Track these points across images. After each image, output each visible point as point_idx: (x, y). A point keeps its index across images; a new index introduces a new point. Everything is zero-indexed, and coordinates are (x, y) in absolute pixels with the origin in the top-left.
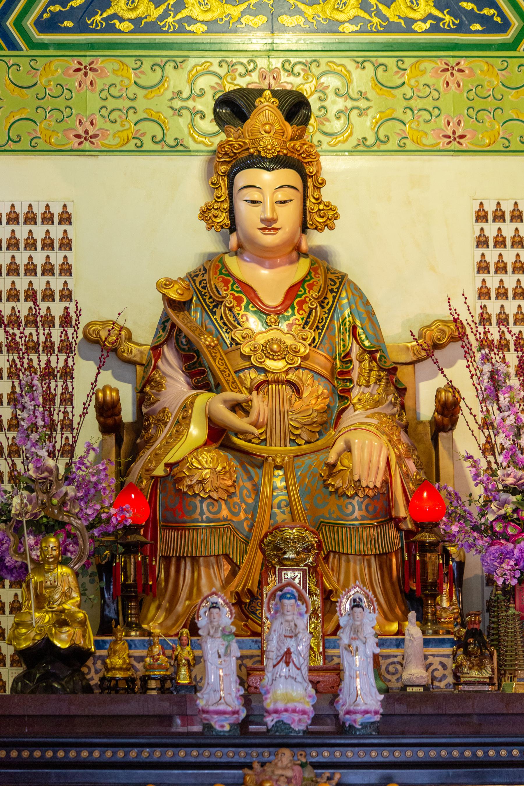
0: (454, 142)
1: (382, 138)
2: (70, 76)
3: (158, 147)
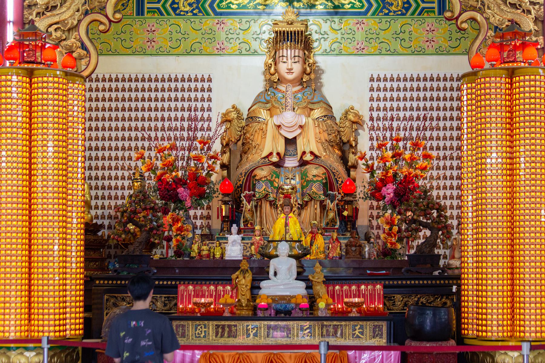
0: (360, 52)
3: (248, 53)
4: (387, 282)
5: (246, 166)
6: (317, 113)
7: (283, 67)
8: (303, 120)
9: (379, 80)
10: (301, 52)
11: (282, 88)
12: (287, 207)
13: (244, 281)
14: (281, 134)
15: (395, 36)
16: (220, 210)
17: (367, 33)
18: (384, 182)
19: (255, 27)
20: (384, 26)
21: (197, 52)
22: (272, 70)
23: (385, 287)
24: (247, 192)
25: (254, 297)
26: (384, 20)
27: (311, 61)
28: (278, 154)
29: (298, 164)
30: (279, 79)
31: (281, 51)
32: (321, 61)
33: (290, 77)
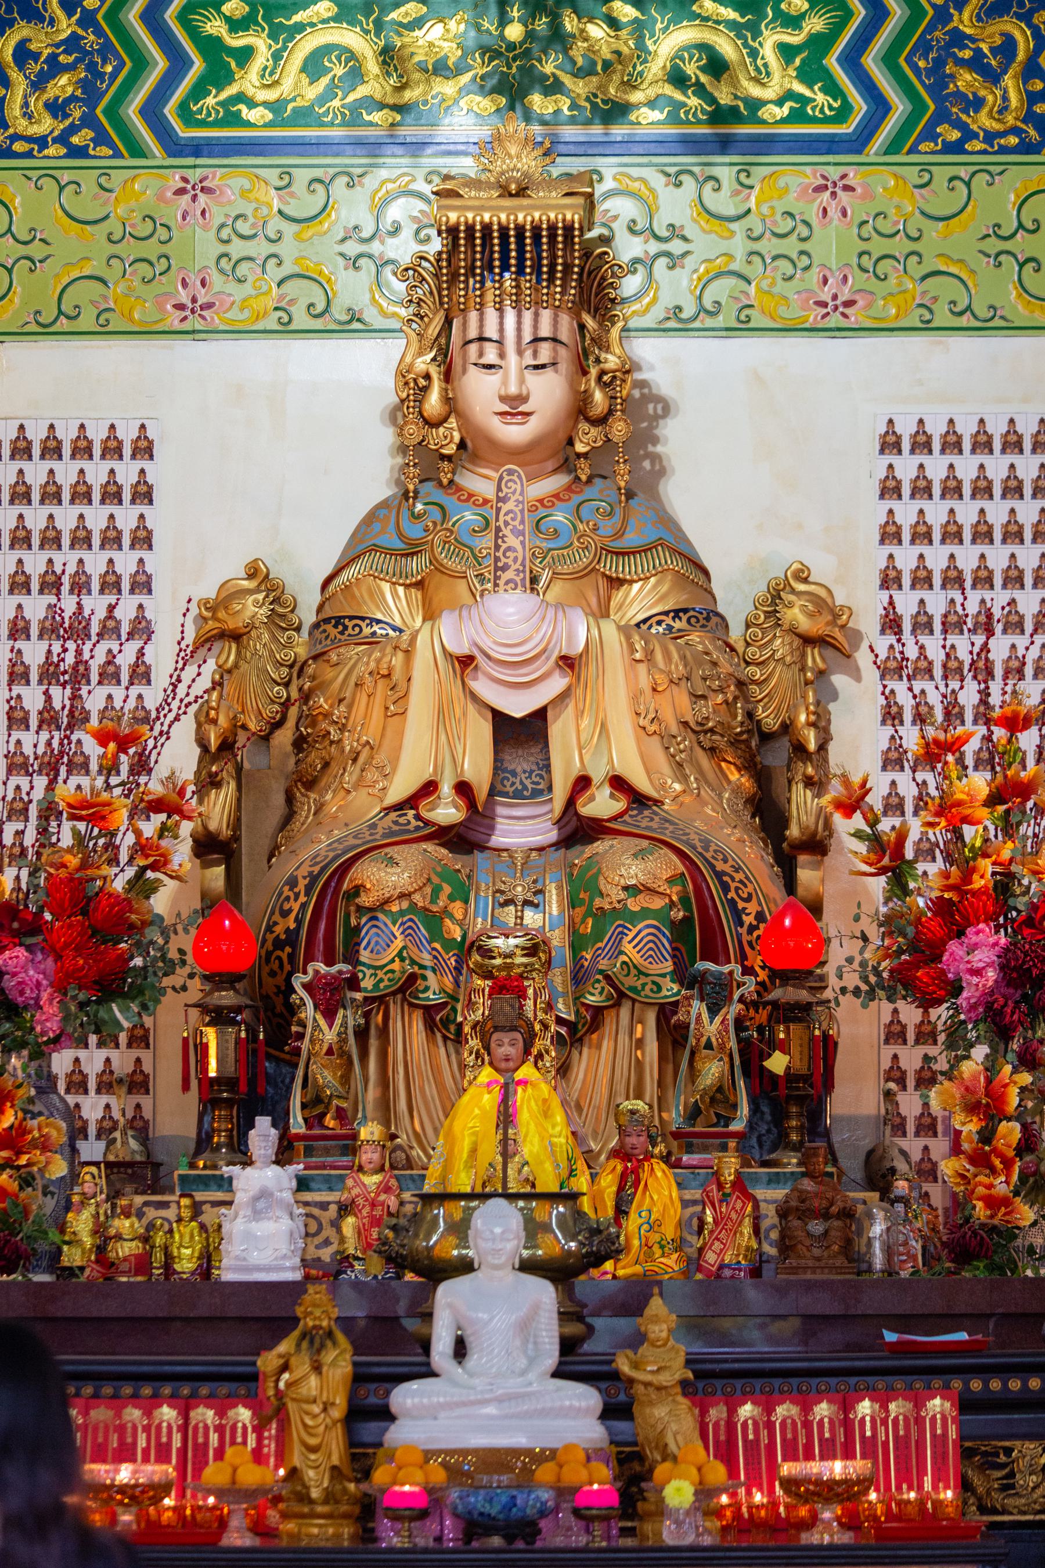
0: (835, 317)
1: (709, 306)
2: (166, 202)
4: (976, 1385)
6: (640, 599)
7: (482, 391)
8: (578, 631)
9: (922, 444)
10: (565, 319)
11: (479, 482)
12: (506, 1037)
13: (317, 1384)
14: (474, 697)
15: (994, 245)
16: (194, 1051)
17: (866, 231)
18: (953, 915)
19: (352, 208)
21: (86, 322)
22: (434, 402)
23: (966, 1405)
24: (322, 968)
25: (362, 1456)
26: (941, 175)
27: (611, 361)
28: (463, 789)
29: (553, 835)
30: (462, 445)
31: (473, 316)
32: (659, 359)
33: (515, 433)
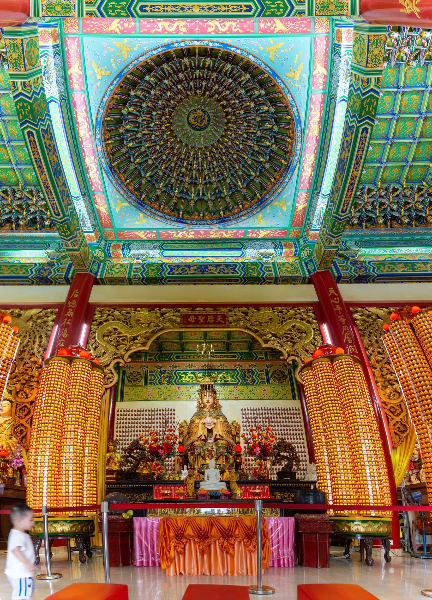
0: (236, 399)
5: (190, 441)
7: (205, 400)
8: (215, 421)
11: (205, 410)
20: (245, 388)
32: (221, 402)
